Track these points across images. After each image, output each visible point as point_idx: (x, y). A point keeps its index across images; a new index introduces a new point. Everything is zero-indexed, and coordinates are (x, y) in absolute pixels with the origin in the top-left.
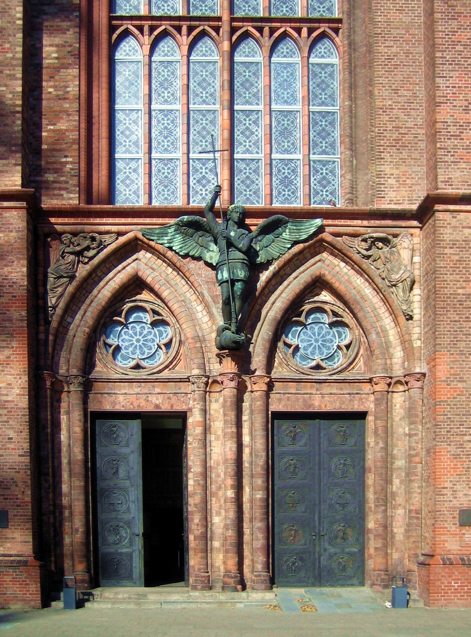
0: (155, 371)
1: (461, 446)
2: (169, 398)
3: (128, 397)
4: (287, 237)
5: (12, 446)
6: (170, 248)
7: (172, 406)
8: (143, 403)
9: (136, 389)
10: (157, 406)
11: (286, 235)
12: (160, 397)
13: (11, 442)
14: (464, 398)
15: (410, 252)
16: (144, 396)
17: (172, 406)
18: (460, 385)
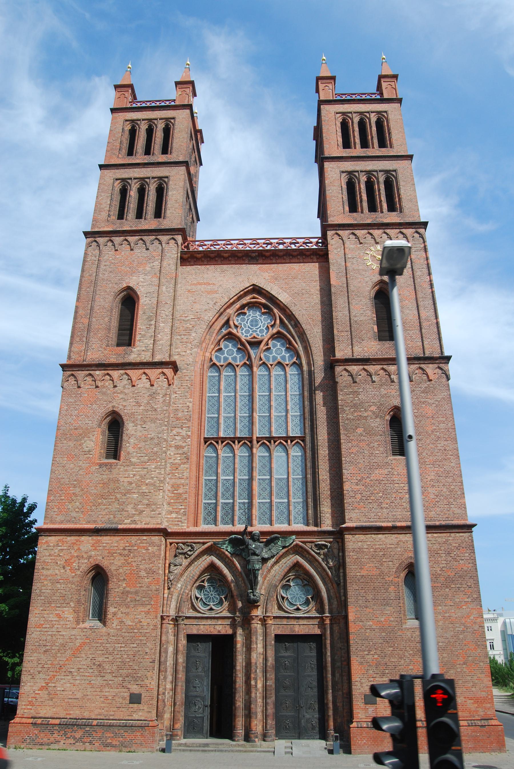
0: (218, 612)
1: (363, 657)
2: (225, 627)
3: (205, 626)
4: (280, 544)
5: (147, 657)
6: (227, 550)
7: (226, 632)
8: (212, 630)
9: (209, 622)
10: (219, 631)
11: (279, 543)
12: (221, 626)
13: (146, 655)
14: (363, 630)
15: (338, 551)
16: (213, 626)
17: (226, 632)
18: (361, 623)
